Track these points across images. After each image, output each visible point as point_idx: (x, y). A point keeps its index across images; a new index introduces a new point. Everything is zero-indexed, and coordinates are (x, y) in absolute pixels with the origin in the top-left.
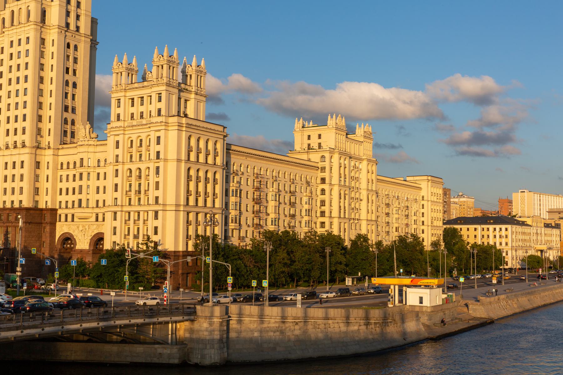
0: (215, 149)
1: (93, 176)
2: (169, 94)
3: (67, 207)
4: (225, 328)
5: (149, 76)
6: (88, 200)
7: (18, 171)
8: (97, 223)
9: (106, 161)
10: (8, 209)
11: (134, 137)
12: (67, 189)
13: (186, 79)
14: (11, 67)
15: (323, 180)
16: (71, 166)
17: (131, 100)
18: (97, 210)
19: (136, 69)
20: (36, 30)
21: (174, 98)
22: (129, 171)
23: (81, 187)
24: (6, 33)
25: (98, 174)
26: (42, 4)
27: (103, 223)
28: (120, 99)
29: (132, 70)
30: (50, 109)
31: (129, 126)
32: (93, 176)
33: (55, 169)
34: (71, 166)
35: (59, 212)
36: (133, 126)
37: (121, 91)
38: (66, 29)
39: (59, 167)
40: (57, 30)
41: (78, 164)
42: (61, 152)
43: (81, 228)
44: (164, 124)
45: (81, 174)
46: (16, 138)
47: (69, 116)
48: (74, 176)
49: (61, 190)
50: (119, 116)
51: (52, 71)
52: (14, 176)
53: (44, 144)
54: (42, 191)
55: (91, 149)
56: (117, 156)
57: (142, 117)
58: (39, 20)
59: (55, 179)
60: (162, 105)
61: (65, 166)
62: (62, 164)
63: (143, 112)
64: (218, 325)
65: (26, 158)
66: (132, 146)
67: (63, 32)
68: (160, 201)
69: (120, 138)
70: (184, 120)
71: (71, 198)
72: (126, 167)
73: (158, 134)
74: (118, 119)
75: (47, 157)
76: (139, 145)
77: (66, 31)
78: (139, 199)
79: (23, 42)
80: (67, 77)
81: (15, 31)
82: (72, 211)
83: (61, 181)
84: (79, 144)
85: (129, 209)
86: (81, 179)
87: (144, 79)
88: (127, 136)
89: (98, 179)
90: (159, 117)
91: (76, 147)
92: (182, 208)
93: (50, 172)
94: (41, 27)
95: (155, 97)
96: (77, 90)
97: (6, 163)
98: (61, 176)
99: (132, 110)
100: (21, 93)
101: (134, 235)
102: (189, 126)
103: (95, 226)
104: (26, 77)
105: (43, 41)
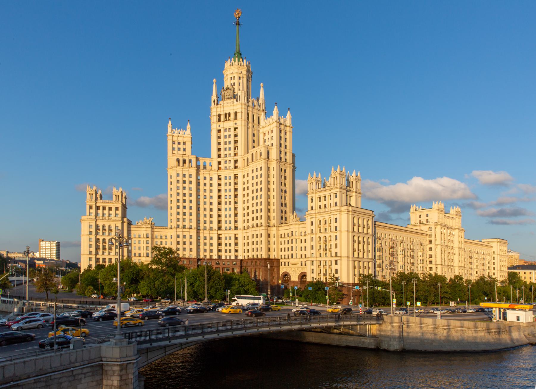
0: (368, 224)
1: (299, 241)
2: (341, 193)
3: (285, 258)
4: (402, 330)
5: (327, 184)
6: (296, 254)
7: (259, 239)
8: (302, 266)
9: (305, 232)
10: (255, 259)
11: (321, 219)
12: (285, 248)
13: (350, 184)
14: (253, 184)
16: (286, 236)
17: (318, 198)
18: (301, 260)
19: (320, 180)
20: (265, 162)
21: (344, 196)
22: (319, 238)
23: (292, 247)
24: (250, 166)
25: (301, 240)
26: (267, 148)
27: (305, 266)
28: (312, 198)
29: (318, 181)
30: (274, 205)
31: (318, 213)
32: (299, 241)
33: (278, 238)
34: (286, 236)
35: (281, 260)
36: (320, 213)
38: (280, 161)
39: (280, 237)
40: (275, 162)
41: (290, 235)
42: (280, 228)
43: (293, 269)
44: (339, 211)
45: (292, 240)
46: (257, 222)
47: (283, 208)
48: (288, 241)
49: (281, 249)
50: (312, 207)
51: (274, 184)
52: (257, 241)
53: (271, 225)
54: (272, 250)
55: (297, 226)
56: (312, 230)
57: (325, 207)
58: (266, 157)
59: (278, 243)
60: (338, 200)
61: (283, 236)
62: (281, 235)
63: (326, 205)
64: (398, 328)
65: (264, 232)
66: (320, 224)
67: (279, 162)
68: (338, 255)
69: (313, 220)
70: (350, 208)
71: (287, 253)
72: (318, 235)
73: (336, 217)
74: (312, 209)
75: (273, 231)
76: (324, 223)
77: (280, 162)
78: (326, 254)
79: (259, 169)
80: (282, 187)
81: (254, 164)
82: (288, 260)
83: (281, 244)
84: (290, 223)
85: (320, 259)
86: (292, 243)
87: (324, 186)
88: (317, 219)
89: (301, 243)
90: (336, 207)
91: (288, 225)
92: (351, 259)
93: (275, 239)
94: (268, 161)
95: (333, 196)
96: (287, 194)
97: (253, 235)
98: (281, 241)
99: (320, 203)
100: (259, 197)
101: (324, 273)
102: (353, 211)
103: (301, 268)
104: (261, 188)
105: (268, 168)
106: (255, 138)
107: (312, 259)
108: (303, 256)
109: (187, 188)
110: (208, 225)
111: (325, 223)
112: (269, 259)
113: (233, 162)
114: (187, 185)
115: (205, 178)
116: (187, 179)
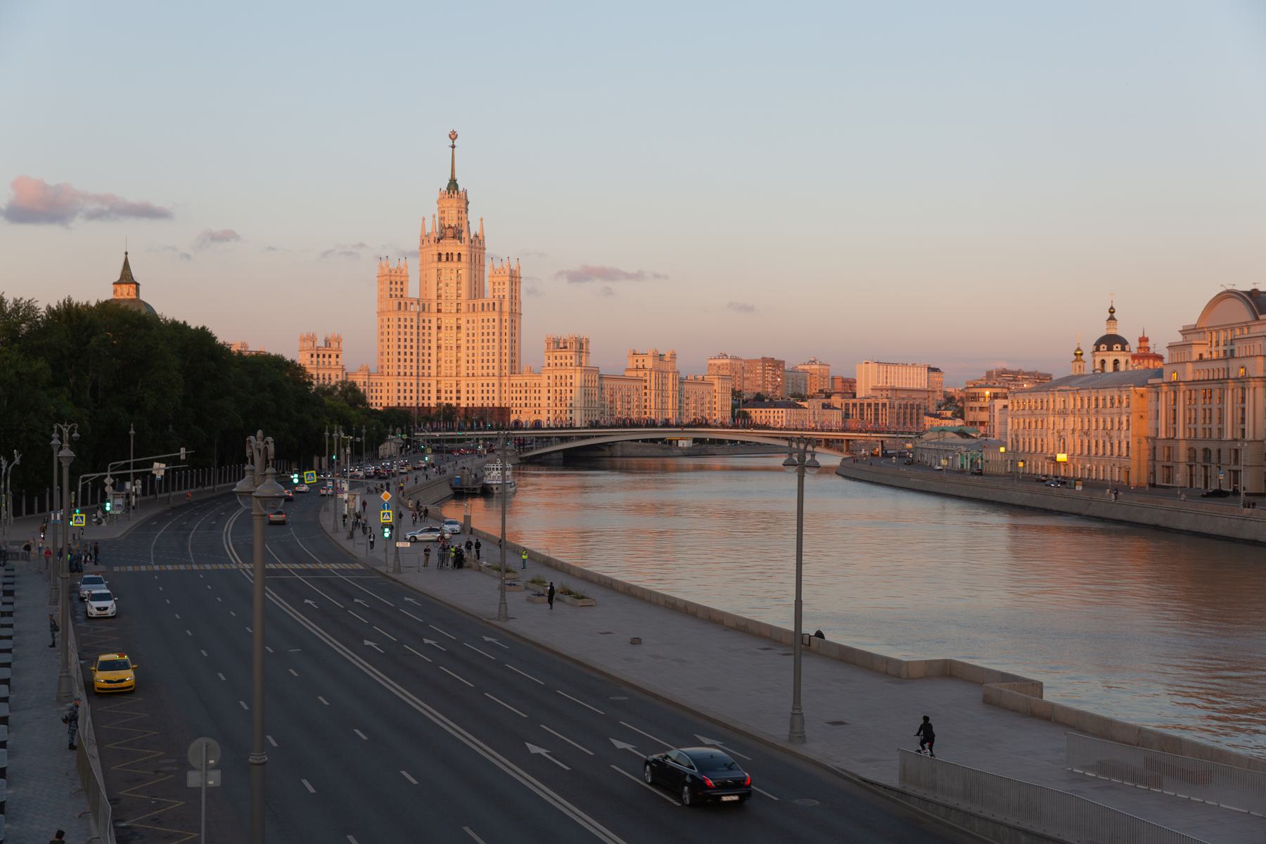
1: (533, 391)
2: (576, 355)
15: (646, 387)
16: (519, 385)
18: (535, 408)
34: (519, 385)
35: (512, 409)
37: (550, 352)
42: (511, 378)
60: (573, 361)
61: (514, 386)
68: (573, 405)
69: (551, 375)
70: (583, 368)
71: (518, 402)
78: (561, 404)
85: (556, 408)
89: (535, 392)
93: (507, 388)
106: (477, 279)
107: (549, 408)
108: (537, 405)
109: (408, 333)
110: (426, 371)
111: (561, 378)
112: (500, 408)
113: (455, 305)
114: (408, 330)
115: (424, 321)
116: (408, 323)
